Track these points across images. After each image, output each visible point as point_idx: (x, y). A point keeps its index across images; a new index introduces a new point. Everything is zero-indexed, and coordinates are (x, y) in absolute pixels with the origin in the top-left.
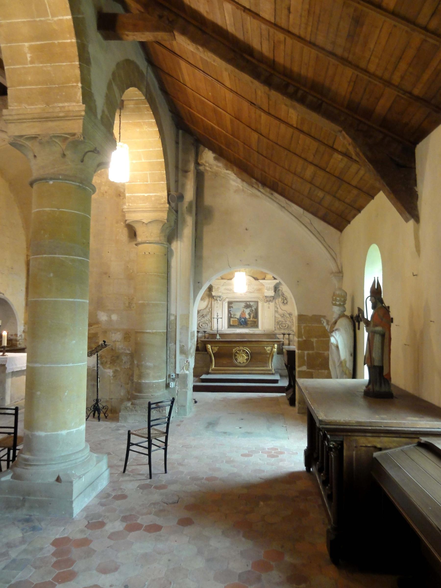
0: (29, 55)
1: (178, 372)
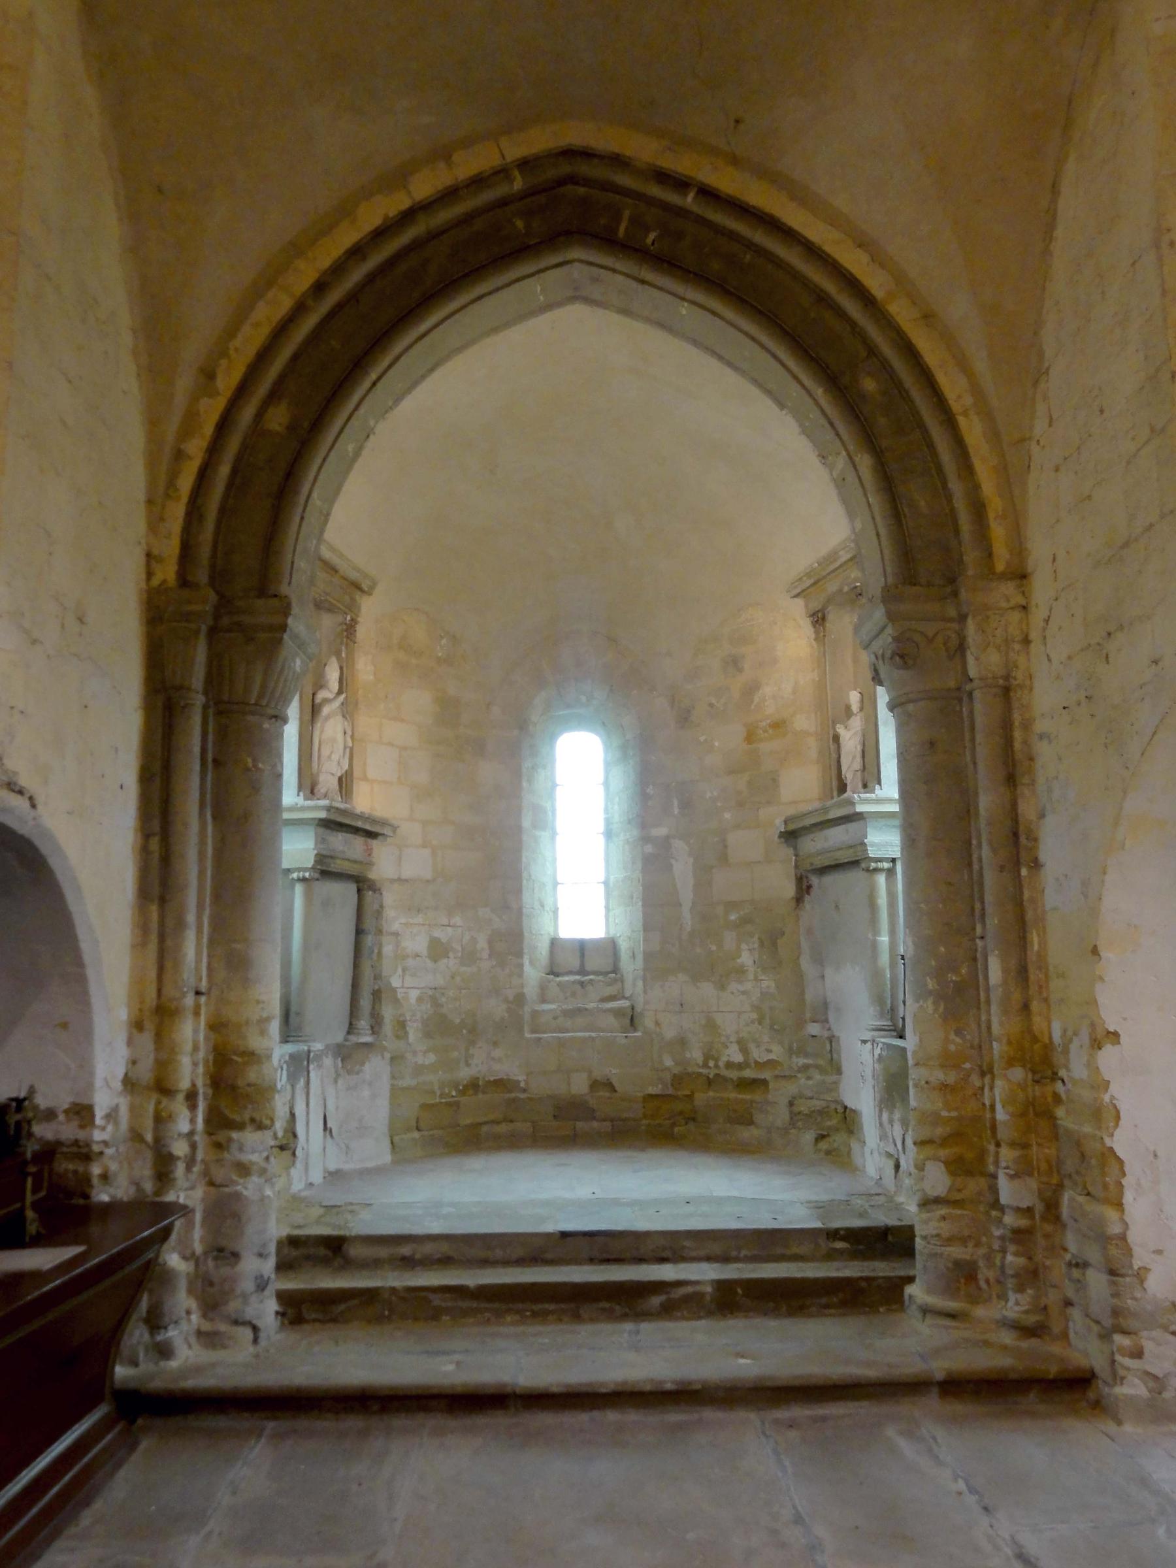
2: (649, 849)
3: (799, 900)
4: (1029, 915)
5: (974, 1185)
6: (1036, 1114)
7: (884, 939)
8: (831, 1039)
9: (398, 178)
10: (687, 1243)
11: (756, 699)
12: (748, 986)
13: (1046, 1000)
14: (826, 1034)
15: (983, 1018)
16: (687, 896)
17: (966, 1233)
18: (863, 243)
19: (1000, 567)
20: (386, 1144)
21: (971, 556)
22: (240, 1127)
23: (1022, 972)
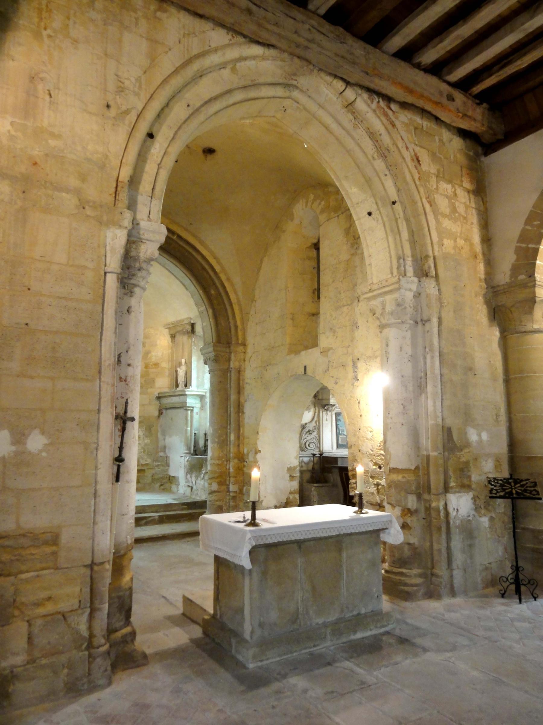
3: (159, 417)
4: (241, 424)
5: (224, 488)
6: (239, 470)
7: (189, 429)
8: (167, 457)
10: (147, 508)
11: (149, 356)
13: (243, 444)
14: (165, 455)
15: (228, 448)
17: (221, 498)
18: (215, 258)
19: (240, 342)
21: (234, 339)
23: (238, 437)
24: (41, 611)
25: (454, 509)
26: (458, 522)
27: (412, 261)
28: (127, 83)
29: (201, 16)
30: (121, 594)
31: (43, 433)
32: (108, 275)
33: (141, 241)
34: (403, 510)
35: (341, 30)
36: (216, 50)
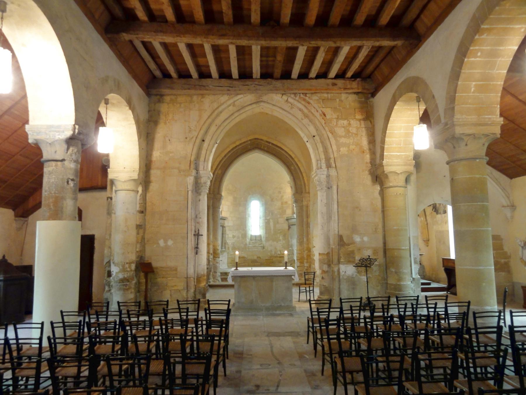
0: (473, 90)
1: (414, 277)
2: (266, 221)
9: (235, 142)
12: (281, 242)
16: (272, 228)
18: (292, 151)
19: (307, 192)
20: (227, 265)
21: (304, 190)
22: (216, 258)
24: (173, 288)
25: (343, 271)
26: (345, 277)
27: (325, 161)
28: (192, 128)
29: (217, 94)
30: (200, 289)
31: (172, 240)
32: (189, 192)
33: (201, 177)
34: (322, 271)
35: (270, 80)
36: (223, 104)
